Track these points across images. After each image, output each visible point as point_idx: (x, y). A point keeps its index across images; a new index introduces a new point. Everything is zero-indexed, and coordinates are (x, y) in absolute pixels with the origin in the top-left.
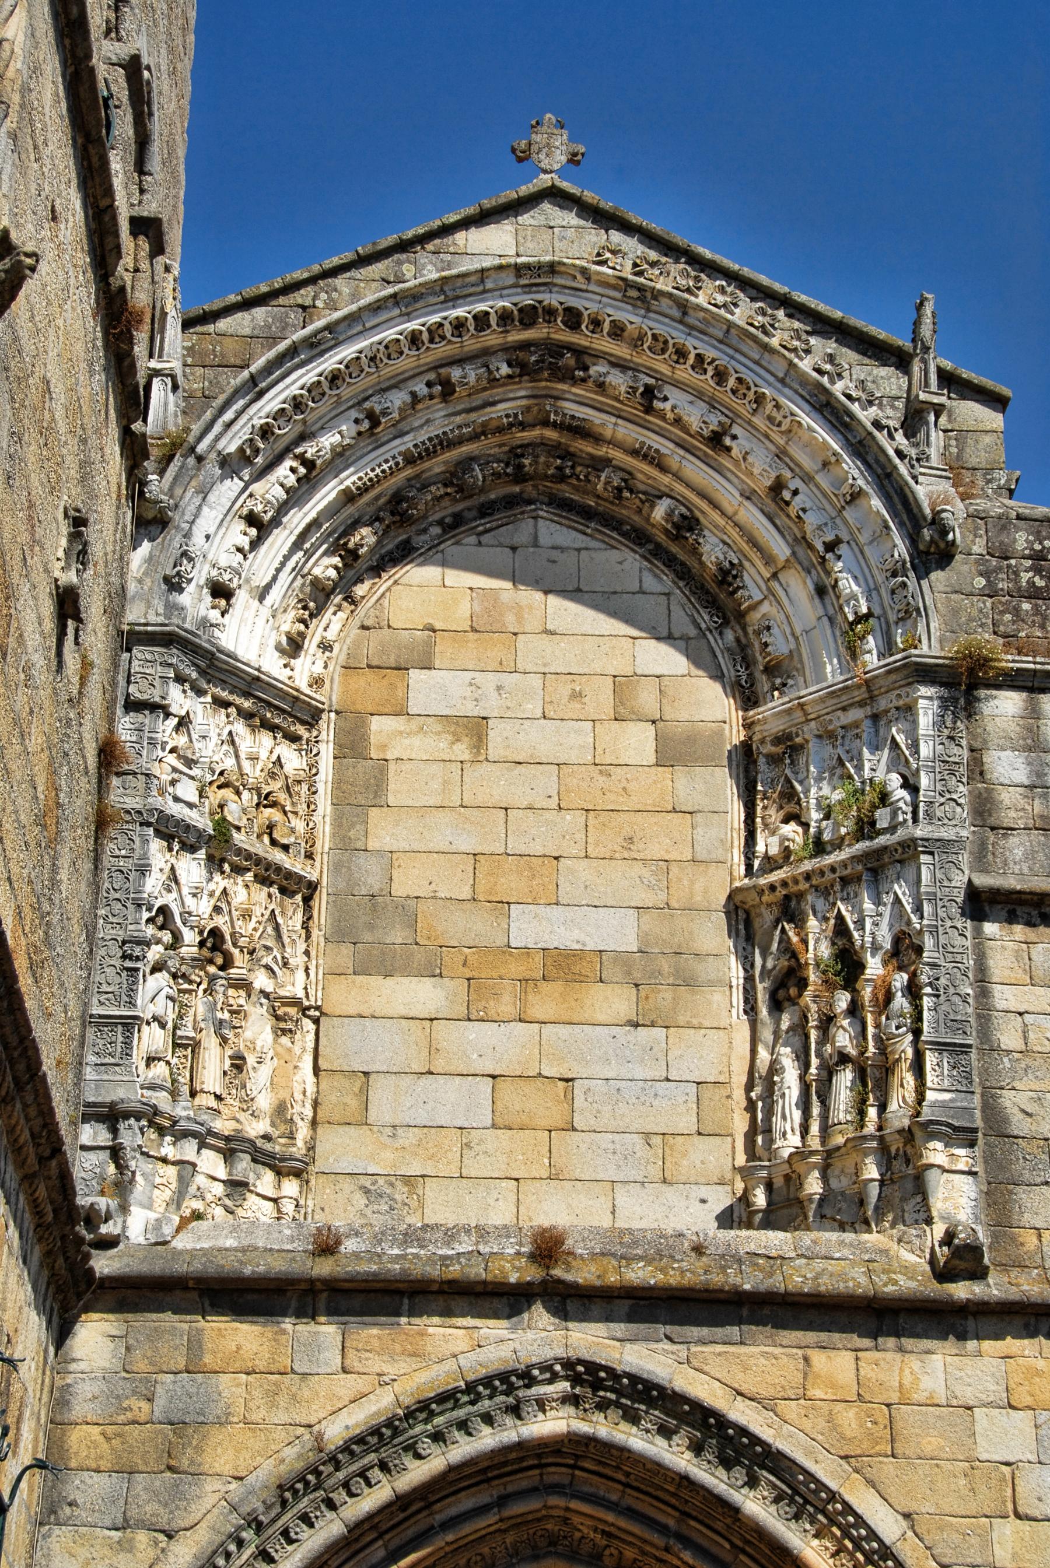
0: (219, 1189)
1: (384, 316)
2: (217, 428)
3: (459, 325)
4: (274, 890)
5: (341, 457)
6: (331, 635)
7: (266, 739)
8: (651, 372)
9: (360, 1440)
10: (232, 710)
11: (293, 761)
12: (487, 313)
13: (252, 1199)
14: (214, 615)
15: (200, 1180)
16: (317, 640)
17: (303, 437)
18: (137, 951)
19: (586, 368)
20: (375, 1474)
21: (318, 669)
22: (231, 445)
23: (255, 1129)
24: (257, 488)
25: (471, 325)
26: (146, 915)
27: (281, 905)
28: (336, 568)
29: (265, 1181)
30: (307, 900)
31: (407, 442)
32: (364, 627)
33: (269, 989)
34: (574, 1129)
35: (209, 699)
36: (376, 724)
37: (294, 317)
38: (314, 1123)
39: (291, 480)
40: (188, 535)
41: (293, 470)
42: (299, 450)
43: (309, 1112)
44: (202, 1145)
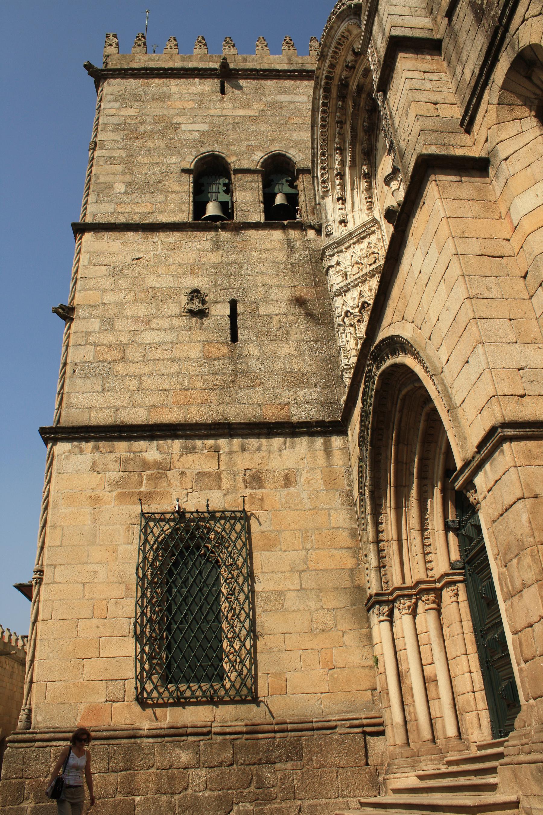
1: (316, 132)
3: (324, 112)
5: (343, 163)
10: (352, 246)
12: (323, 102)
14: (344, 228)
22: (321, 194)
24: (335, 193)
28: (366, 182)
31: (349, 141)
35: (344, 250)
39: (337, 182)
40: (327, 221)
41: (337, 179)
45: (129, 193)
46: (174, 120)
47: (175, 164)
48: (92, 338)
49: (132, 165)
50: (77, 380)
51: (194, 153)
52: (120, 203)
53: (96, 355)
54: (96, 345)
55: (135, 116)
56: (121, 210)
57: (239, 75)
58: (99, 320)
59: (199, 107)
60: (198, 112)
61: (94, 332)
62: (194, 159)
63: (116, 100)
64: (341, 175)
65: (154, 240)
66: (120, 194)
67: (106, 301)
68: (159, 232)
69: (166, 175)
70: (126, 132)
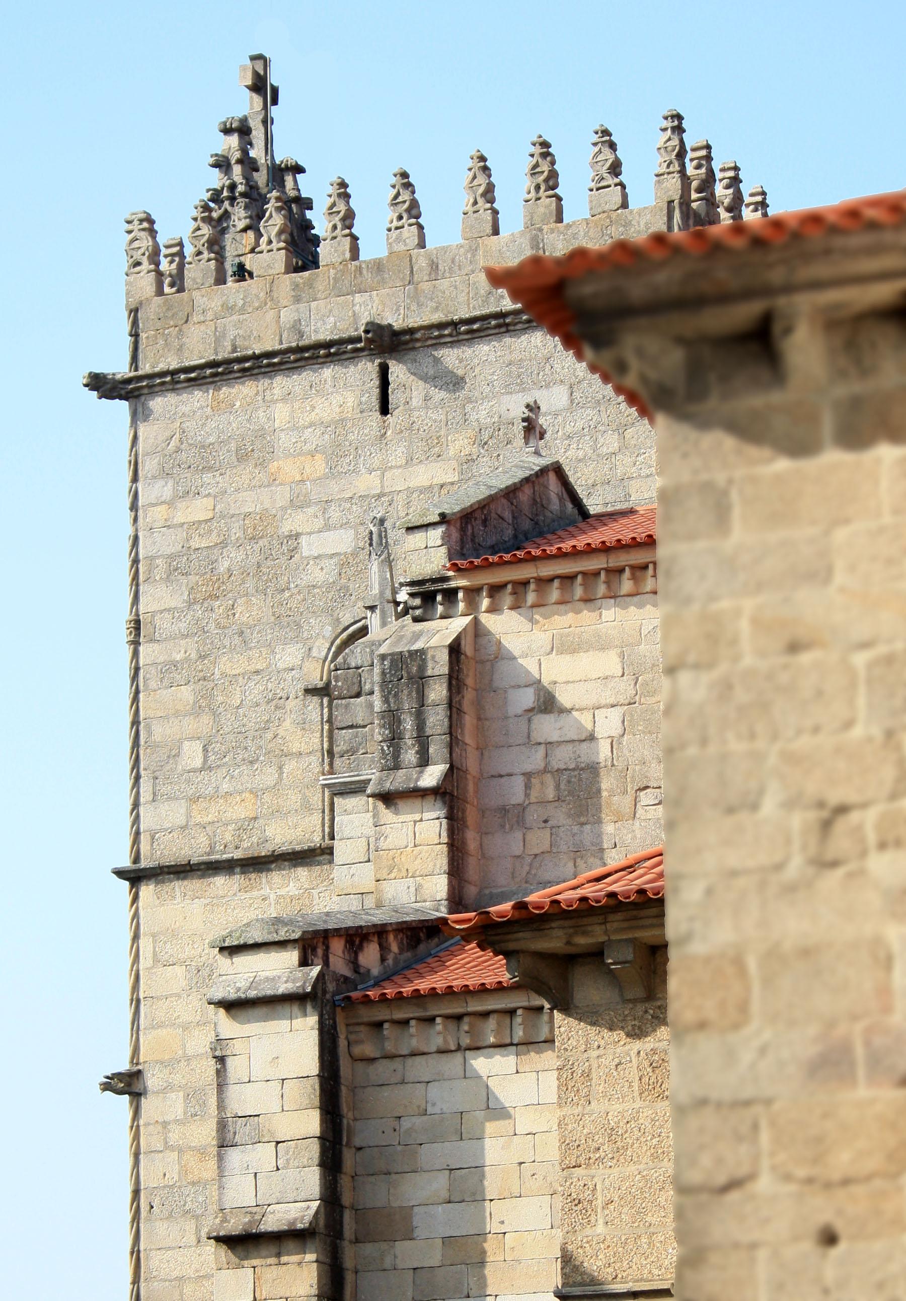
45: (210, 768)
46: (286, 528)
47: (293, 670)
48: (174, 1137)
49: (212, 684)
50: (157, 1223)
51: (328, 631)
52: (194, 799)
53: (184, 1170)
54: (181, 1151)
55: (206, 521)
56: (198, 819)
57: (417, 340)
58: (181, 1094)
59: (333, 473)
60: (333, 488)
61: (176, 1121)
62: (329, 649)
63: (165, 474)
65: (262, 892)
66: (194, 771)
67: (190, 1052)
68: (269, 870)
69: (277, 707)
70: (193, 579)
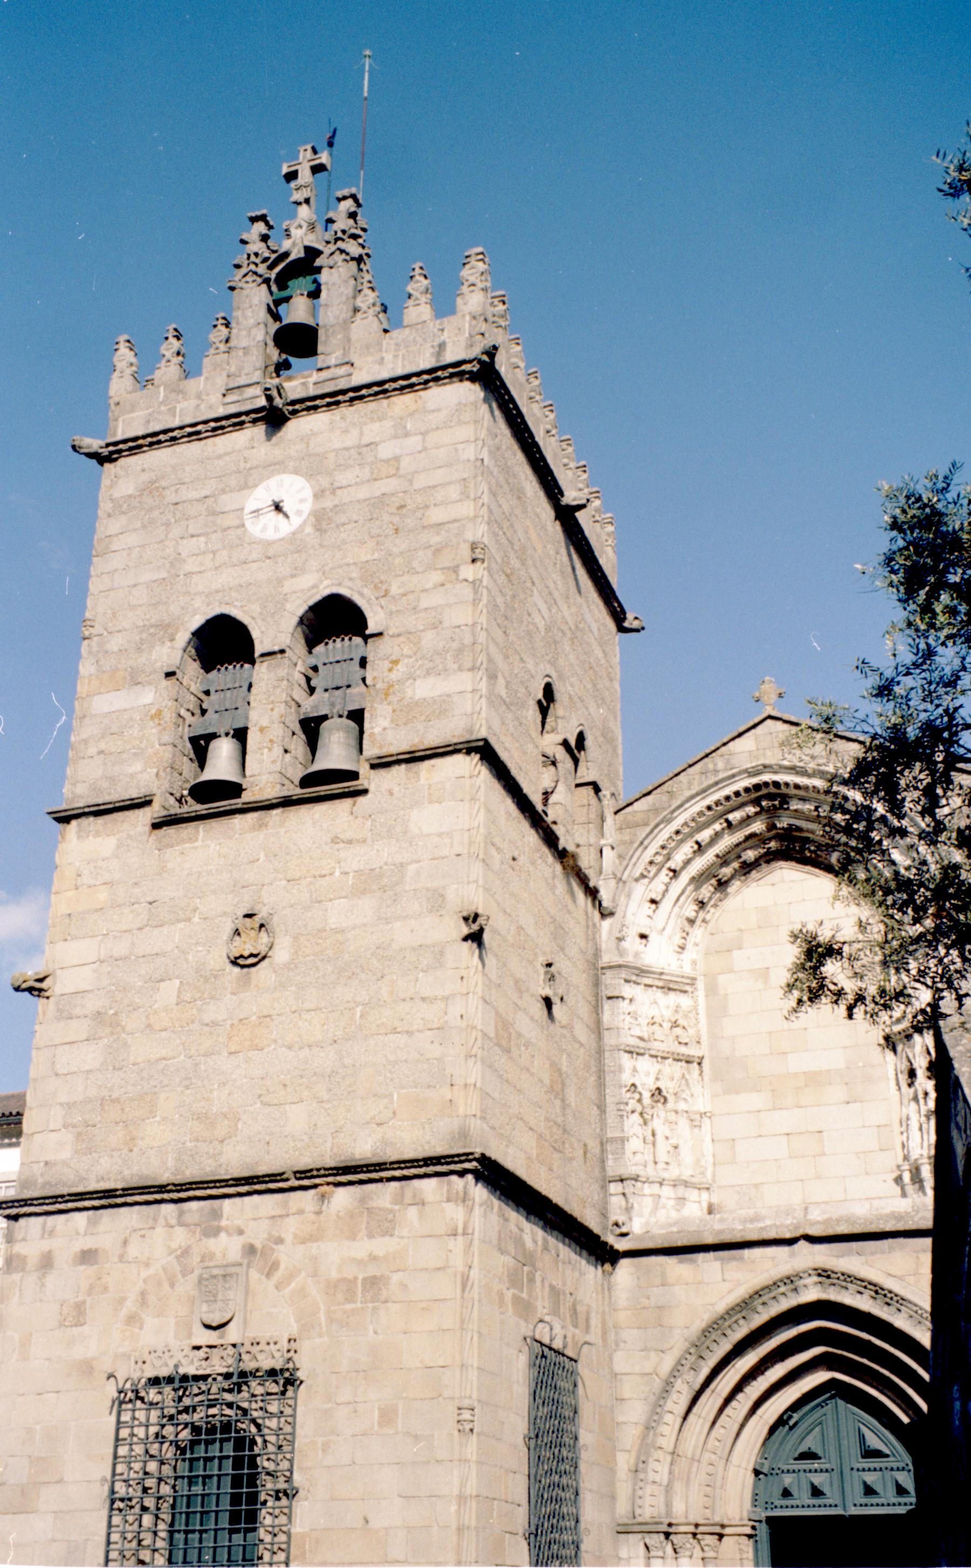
0: (672, 1203)
2: (629, 868)
3: (728, 798)
4: (683, 1064)
5: (687, 862)
6: (698, 940)
7: (672, 995)
8: (816, 800)
9: (733, 1309)
11: (684, 1001)
13: (688, 1203)
14: (641, 948)
15: (663, 1200)
16: (692, 943)
17: (668, 859)
18: (622, 1107)
19: (788, 803)
20: (742, 1322)
21: (694, 956)
23: (686, 1175)
25: (733, 796)
26: (624, 1090)
27: (688, 1070)
29: (693, 1194)
30: (699, 1064)
32: (712, 934)
33: (686, 1109)
34: (825, 1154)
36: (722, 979)
37: (665, 798)
38: (714, 1164)
39: (667, 880)
42: (668, 865)
43: (711, 1160)
44: (661, 1184)
64: (675, 873)
